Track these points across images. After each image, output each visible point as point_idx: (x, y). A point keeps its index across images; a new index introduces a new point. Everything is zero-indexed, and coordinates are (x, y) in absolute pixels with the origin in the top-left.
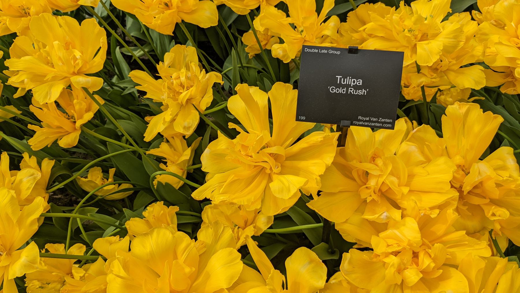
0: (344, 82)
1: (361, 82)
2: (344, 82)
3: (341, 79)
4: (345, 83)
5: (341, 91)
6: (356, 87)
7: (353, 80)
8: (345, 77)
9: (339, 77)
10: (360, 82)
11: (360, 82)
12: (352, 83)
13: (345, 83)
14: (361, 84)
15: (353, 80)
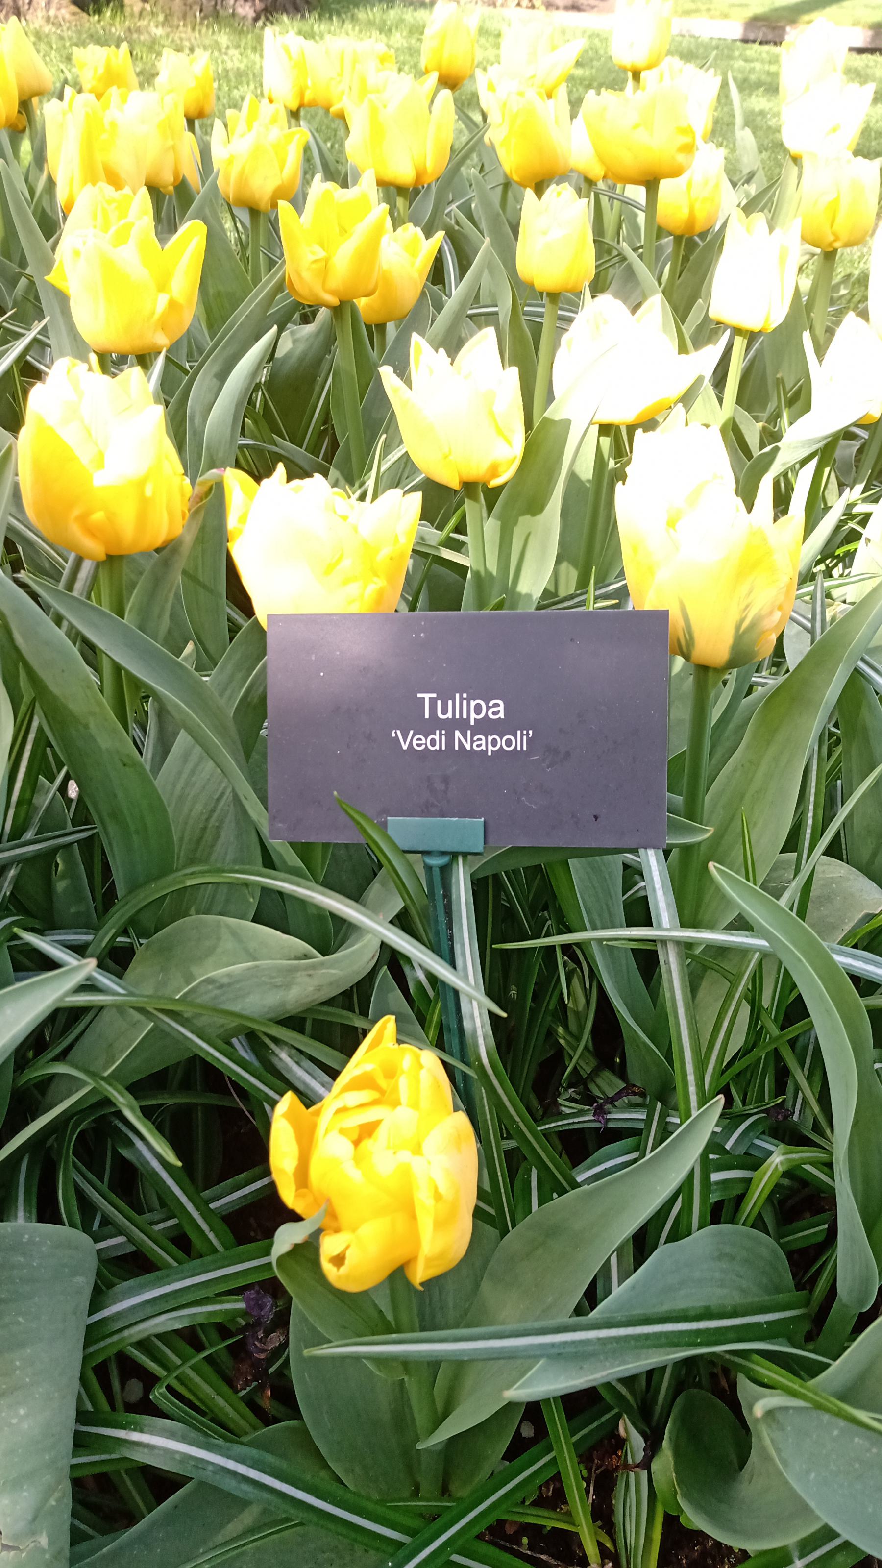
0: (445, 711)
1: (501, 708)
2: (445, 711)
3: (433, 702)
4: (449, 715)
5: (437, 741)
6: (485, 727)
7: (473, 703)
8: (445, 696)
9: (427, 696)
10: (498, 709)
11: (498, 709)
12: (473, 716)
13: (449, 715)
14: (501, 715)
15: (473, 703)
